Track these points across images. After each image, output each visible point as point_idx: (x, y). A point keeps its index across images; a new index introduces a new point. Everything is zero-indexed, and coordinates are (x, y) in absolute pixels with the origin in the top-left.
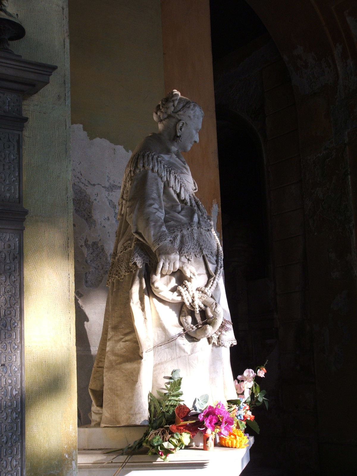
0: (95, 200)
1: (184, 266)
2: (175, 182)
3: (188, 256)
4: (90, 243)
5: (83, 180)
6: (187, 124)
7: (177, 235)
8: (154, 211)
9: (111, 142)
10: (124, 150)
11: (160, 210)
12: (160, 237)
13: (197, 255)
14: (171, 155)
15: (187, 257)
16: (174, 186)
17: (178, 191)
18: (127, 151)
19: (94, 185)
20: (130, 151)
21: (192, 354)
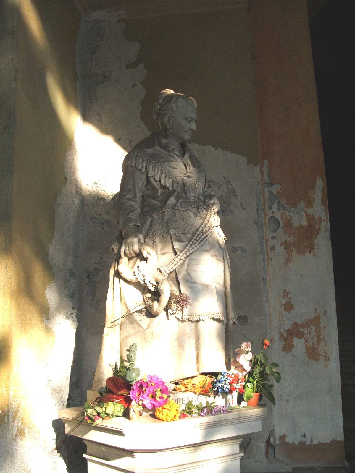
1: (141, 247)
2: (154, 172)
3: (152, 238)
6: (173, 117)
7: (147, 220)
8: (126, 201)
9: (200, 144)
10: (213, 148)
11: (134, 199)
12: (126, 223)
13: (164, 235)
14: (155, 148)
15: (152, 239)
16: (153, 175)
17: (157, 179)
18: (216, 149)
20: (219, 148)
21: (147, 329)
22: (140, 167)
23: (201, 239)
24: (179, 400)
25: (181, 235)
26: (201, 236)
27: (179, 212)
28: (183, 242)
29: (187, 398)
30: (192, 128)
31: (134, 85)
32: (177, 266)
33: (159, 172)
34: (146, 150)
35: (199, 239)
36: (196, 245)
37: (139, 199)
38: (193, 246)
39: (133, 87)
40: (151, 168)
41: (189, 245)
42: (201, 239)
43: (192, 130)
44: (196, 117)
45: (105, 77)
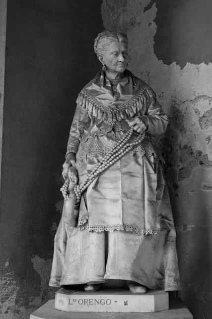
0: (185, 113)
4: (182, 146)
5: (177, 102)
18: (208, 64)
19: (184, 102)
22: (81, 104)
23: (110, 159)
24: (86, 301)
25: (94, 158)
26: (110, 157)
27: (98, 138)
28: (95, 163)
29: (95, 300)
30: (119, 60)
31: (150, 24)
32: (87, 185)
33: (92, 105)
34: (87, 88)
35: (108, 160)
36: (103, 165)
37: (79, 130)
38: (100, 167)
39: (149, 26)
40: (87, 103)
41: (97, 166)
42: (110, 159)
43: (120, 62)
44: (123, 49)
45: (132, 24)
